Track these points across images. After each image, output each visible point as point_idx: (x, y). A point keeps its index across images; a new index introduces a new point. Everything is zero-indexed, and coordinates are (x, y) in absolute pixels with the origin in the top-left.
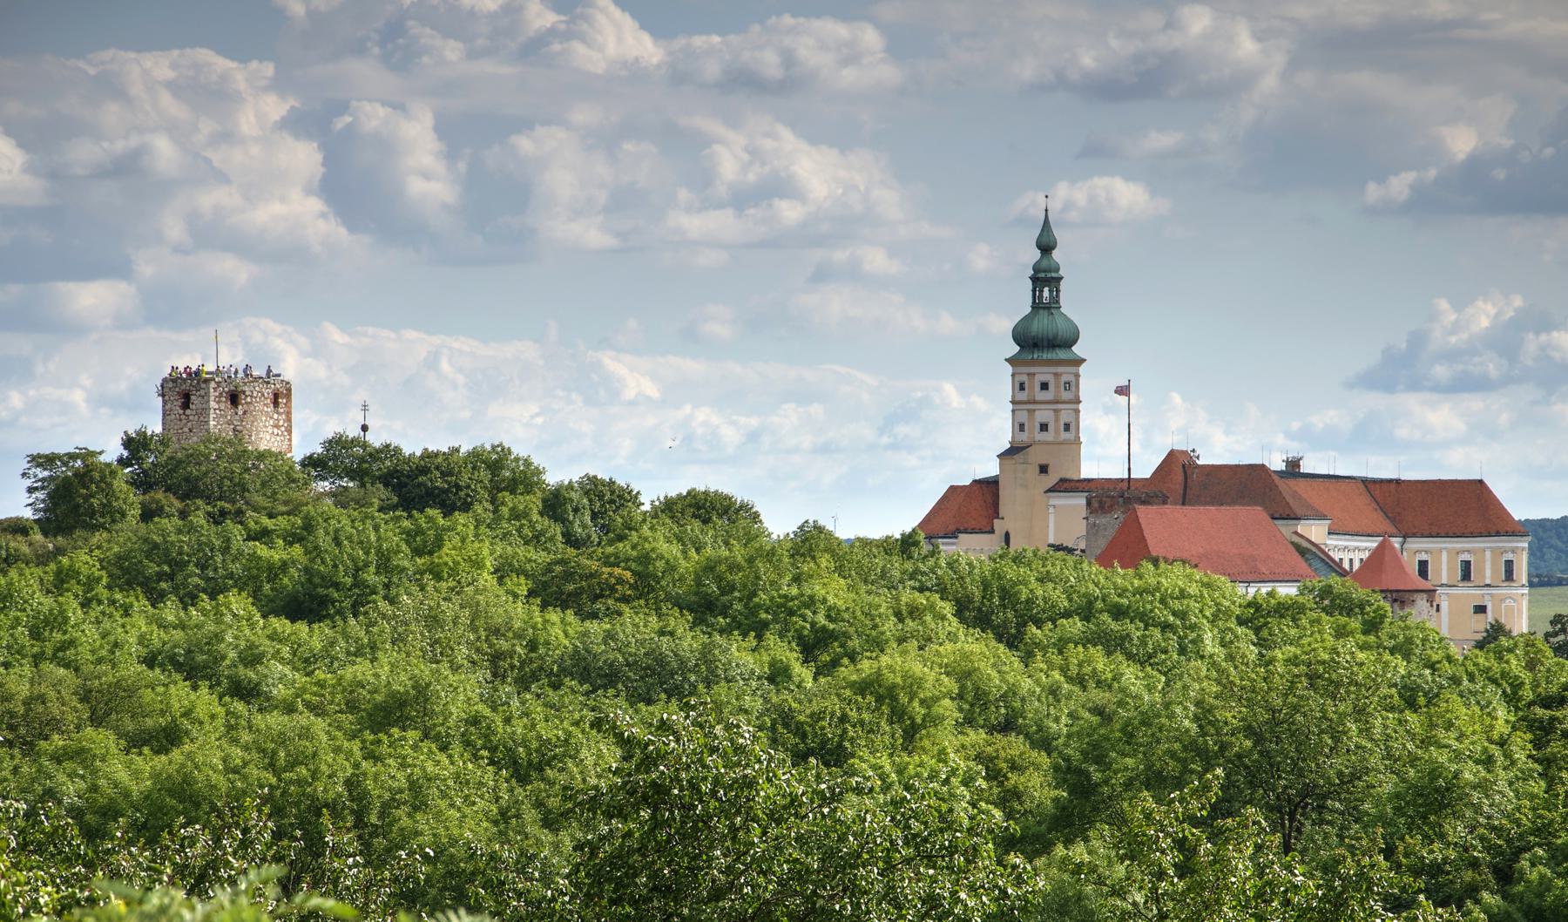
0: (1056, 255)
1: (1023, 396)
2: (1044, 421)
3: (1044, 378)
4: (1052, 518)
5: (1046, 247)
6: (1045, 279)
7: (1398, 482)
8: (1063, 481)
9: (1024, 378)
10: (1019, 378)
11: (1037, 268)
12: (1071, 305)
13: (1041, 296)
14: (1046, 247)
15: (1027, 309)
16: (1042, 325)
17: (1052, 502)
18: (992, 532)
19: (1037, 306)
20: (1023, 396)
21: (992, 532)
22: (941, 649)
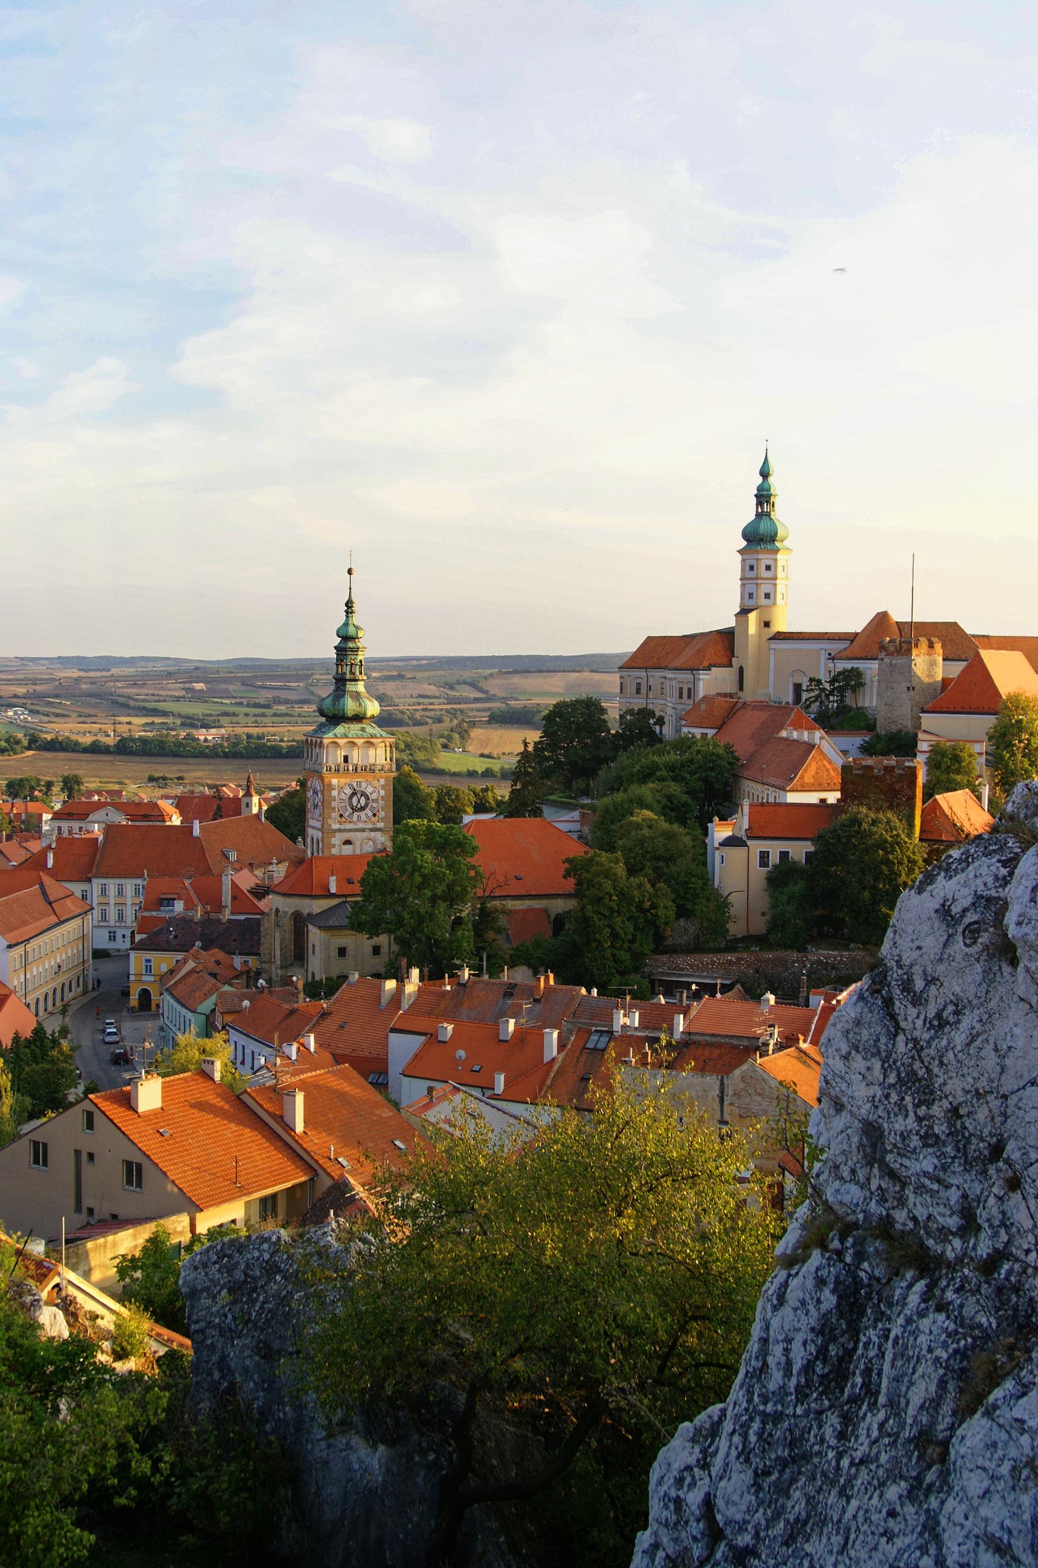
0: (771, 480)
1: (752, 574)
2: (767, 591)
3: (768, 562)
4: (772, 657)
5: (765, 474)
6: (763, 497)
7: (987, 636)
9: (753, 562)
10: (748, 563)
12: (781, 513)
14: (765, 474)
15: (752, 517)
16: (764, 527)
17: (773, 646)
18: (731, 666)
19: (758, 515)
20: (752, 574)
21: (731, 666)
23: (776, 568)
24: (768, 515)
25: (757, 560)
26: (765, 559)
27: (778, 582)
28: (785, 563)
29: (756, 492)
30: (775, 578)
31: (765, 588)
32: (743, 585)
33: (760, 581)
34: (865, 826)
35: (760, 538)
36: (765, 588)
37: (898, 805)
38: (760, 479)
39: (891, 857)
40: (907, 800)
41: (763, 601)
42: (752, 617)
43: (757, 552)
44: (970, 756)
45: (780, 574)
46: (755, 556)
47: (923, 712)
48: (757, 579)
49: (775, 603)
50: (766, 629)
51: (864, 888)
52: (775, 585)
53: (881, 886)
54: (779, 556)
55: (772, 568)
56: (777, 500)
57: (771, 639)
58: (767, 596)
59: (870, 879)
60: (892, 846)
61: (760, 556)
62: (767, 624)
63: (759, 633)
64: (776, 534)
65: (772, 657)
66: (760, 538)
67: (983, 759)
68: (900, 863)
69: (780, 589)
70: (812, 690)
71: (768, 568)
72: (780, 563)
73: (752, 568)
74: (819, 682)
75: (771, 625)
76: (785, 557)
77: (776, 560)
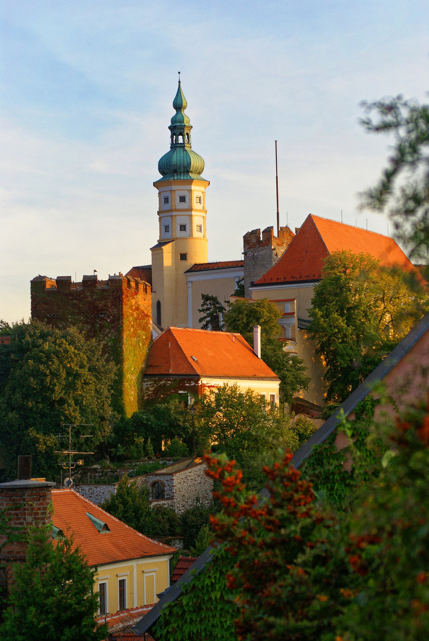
0: (186, 112)
1: (167, 207)
2: (183, 223)
3: (183, 194)
4: (190, 290)
5: (178, 106)
6: (178, 128)
8: (196, 265)
9: (168, 194)
11: (174, 120)
12: (199, 144)
13: (177, 139)
14: (178, 106)
15: (168, 149)
16: (177, 158)
17: (190, 279)
19: (174, 146)
22: (336, 315)
23: (191, 199)
24: (182, 146)
25: (171, 191)
26: (179, 190)
27: (193, 213)
28: (201, 195)
29: (170, 124)
30: (191, 210)
31: (180, 220)
32: (160, 218)
33: (174, 213)
34: (28, 338)
35: (176, 171)
36: (180, 220)
37: (102, 327)
38: (174, 112)
39: (42, 367)
40: (112, 322)
41: (179, 234)
42: (167, 249)
43: (170, 184)
44: (270, 311)
45: (196, 205)
46: (167, 188)
47: (253, 285)
48: (171, 211)
49: (191, 235)
50: (183, 262)
51: (13, 409)
52: (191, 216)
53: (30, 404)
54: (194, 187)
55: (187, 199)
56: (192, 133)
57: (188, 271)
58: (183, 228)
59: (18, 397)
60: (48, 357)
61: (174, 188)
62: (184, 257)
63: (176, 267)
64: (189, 164)
65: (190, 290)
66: (176, 171)
67: (295, 321)
68: (54, 375)
69: (197, 220)
70: (208, 309)
71: (183, 199)
72: (195, 195)
73: (166, 200)
74: (214, 300)
75: (188, 257)
76: (202, 189)
77: (190, 191)
